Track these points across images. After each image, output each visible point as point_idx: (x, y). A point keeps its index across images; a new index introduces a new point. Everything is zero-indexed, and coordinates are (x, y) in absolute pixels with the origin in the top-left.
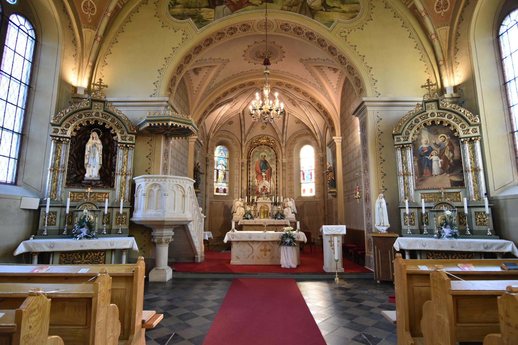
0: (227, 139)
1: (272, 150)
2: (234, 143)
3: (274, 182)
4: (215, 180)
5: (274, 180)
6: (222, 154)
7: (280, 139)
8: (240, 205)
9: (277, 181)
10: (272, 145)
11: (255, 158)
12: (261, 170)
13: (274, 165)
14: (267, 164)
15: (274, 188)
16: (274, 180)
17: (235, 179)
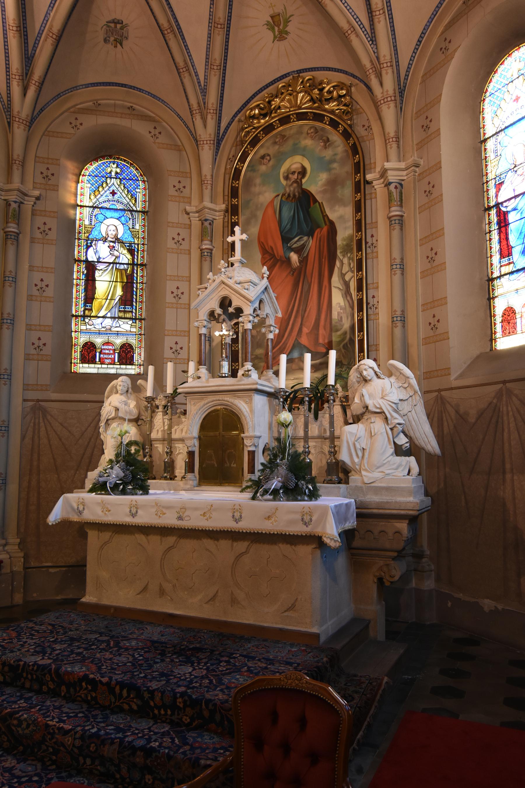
0: (125, 123)
1: (335, 137)
2: (162, 139)
3: (347, 293)
4: (77, 308)
5: (347, 284)
6: (113, 193)
7: (366, 62)
8: (117, 409)
9: (360, 289)
10: (332, 112)
11: (257, 189)
12: (286, 239)
13: (345, 205)
14: (315, 210)
15: (346, 325)
16: (347, 284)
17: (169, 298)
